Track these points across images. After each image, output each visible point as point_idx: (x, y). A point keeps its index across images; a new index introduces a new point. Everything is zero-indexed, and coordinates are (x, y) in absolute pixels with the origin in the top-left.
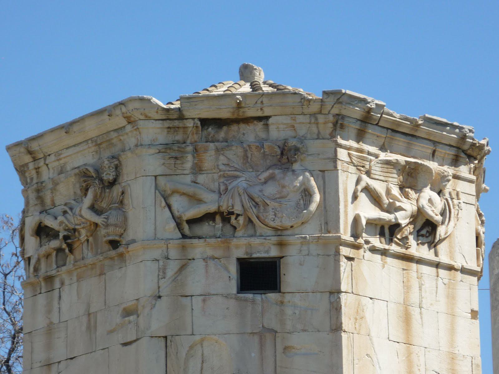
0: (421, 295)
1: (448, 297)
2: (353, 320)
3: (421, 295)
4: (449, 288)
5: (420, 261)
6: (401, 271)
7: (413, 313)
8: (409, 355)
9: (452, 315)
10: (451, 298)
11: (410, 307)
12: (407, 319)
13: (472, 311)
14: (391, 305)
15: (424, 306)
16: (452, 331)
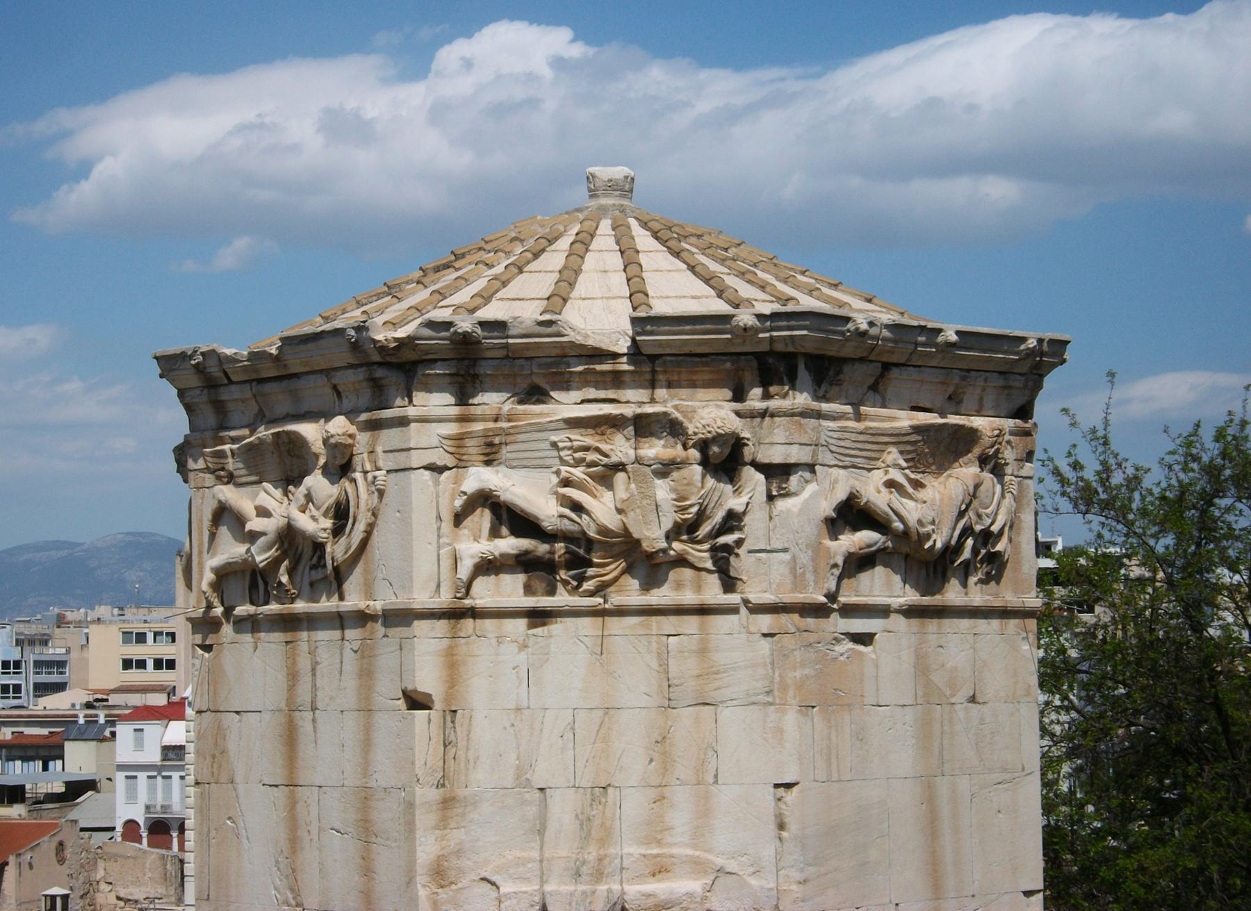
0: (314, 686)
1: (360, 676)
2: (209, 759)
3: (314, 686)
4: (363, 657)
5: (311, 622)
6: (282, 648)
7: (301, 723)
8: (292, 805)
9: (367, 709)
10: (367, 674)
11: (297, 713)
12: (290, 738)
13: (404, 692)
14: (266, 716)
15: (319, 705)
16: (367, 744)
